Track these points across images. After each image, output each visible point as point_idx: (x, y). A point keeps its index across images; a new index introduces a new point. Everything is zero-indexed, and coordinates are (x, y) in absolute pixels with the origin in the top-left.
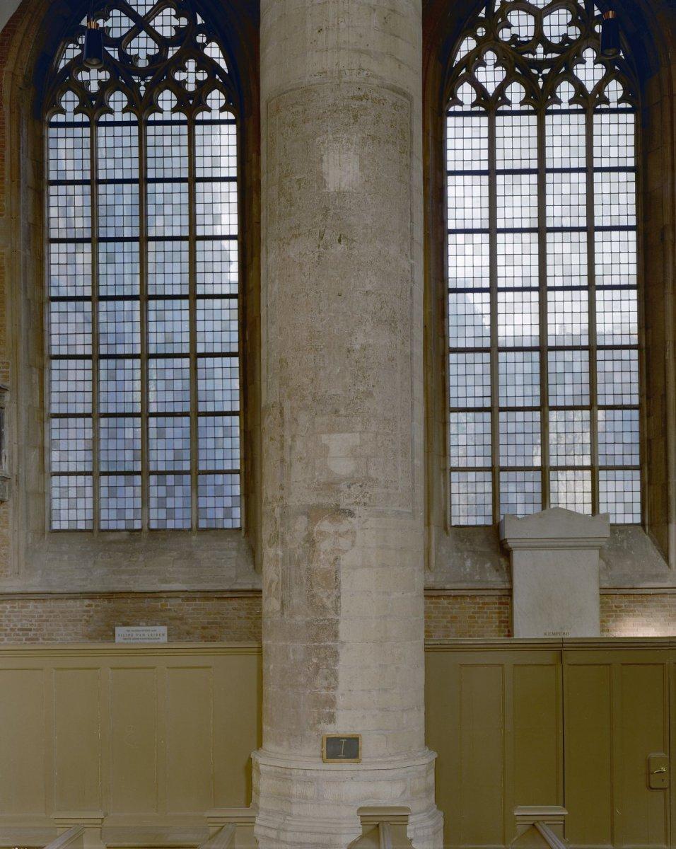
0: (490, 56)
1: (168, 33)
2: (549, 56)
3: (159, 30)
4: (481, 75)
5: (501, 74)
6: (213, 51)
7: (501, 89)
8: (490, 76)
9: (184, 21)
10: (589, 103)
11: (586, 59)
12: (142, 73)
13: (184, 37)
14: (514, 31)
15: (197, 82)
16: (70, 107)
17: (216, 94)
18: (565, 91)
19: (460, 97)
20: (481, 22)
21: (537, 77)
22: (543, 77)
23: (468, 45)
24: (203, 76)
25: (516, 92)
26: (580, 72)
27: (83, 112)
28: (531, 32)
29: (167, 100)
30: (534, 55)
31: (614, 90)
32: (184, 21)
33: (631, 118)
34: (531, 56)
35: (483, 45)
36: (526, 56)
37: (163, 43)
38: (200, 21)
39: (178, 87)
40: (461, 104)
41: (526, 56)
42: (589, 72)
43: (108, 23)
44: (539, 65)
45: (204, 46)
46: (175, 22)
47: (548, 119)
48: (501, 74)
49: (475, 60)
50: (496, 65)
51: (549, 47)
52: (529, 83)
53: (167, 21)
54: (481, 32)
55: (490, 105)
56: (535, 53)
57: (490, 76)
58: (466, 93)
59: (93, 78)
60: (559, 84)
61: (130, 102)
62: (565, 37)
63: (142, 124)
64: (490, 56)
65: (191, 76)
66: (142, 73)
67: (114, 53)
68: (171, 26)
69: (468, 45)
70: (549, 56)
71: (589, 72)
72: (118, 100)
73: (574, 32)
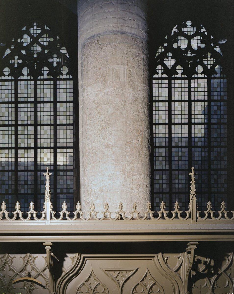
1: (45, 44)
2: (193, 55)
3: (42, 43)
6: (64, 51)
8: (170, 62)
9: (52, 40)
15: (57, 62)
16: (26, 73)
17: (26, 69)
20: (166, 41)
21: (188, 64)
23: (161, 50)
25: (180, 70)
27: (11, 76)
28: (186, 46)
34: (185, 55)
35: (167, 50)
42: (209, 62)
43: (22, 40)
46: (48, 40)
47: (58, 82)
49: (164, 55)
50: (172, 58)
51: (193, 51)
52: (185, 66)
53: (45, 39)
56: (187, 54)
59: (16, 61)
60: (43, 67)
63: (55, 80)
65: (55, 60)
67: (24, 52)
68: (47, 41)
69: (161, 50)
70: (193, 55)
71: (209, 62)
72: (26, 71)
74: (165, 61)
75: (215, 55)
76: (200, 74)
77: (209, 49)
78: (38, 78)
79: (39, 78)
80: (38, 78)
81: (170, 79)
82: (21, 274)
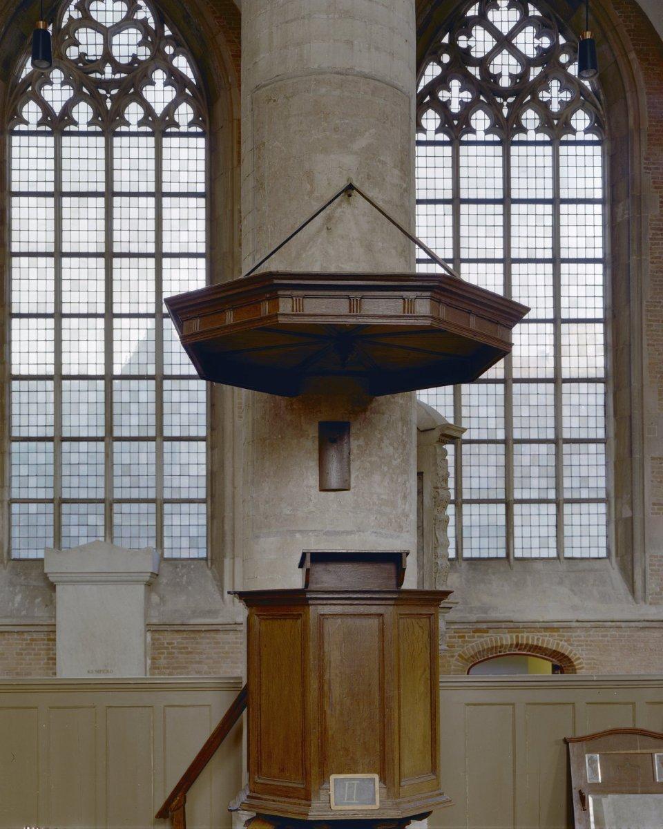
2: (118, 76)
4: (48, 93)
5: (68, 93)
7: (68, 107)
8: (57, 94)
10: (160, 126)
11: (156, 81)
14: (82, 49)
18: (134, 112)
19: (25, 116)
25: (83, 113)
26: (149, 94)
30: (102, 74)
31: (185, 113)
33: (201, 142)
34: (98, 76)
36: (93, 75)
40: (27, 123)
41: (93, 75)
42: (159, 94)
44: (108, 84)
47: (117, 141)
48: (68, 93)
50: (63, 84)
51: (117, 68)
52: (96, 102)
55: (57, 124)
56: (103, 73)
57: (57, 94)
58: (31, 112)
60: (127, 105)
62: (135, 57)
70: (118, 76)
71: (159, 94)
73: (144, 53)
74: (468, 98)
75: (175, 78)
76: (583, 133)
77: (159, 60)
78: (462, 139)
79: (564, 138)
80: (462, 139)
81: (455, 143)
82: (141, 578)
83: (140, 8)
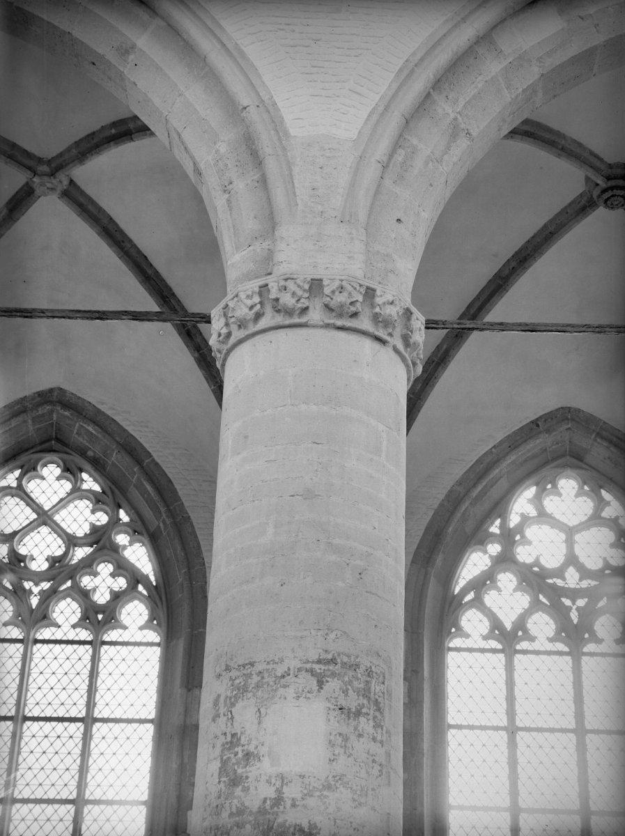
0: (507, 580)
5: (524, 600)
9: (102, 518)
12: (38, 577)
13: (100, 540)
22: (578, 609)
24: (121, 583)
25: (543, 625)
29: (67, 611)
32: (102, 518)
36: (550, 581)
37: (71, 541)
38: (124, 516)
39: (84, 596)
44: (574, 594)
45: (125, 547)
51: (584, 573)
52: (559, 613)
54: (494, 549)
58: (472, 622)
61: (17, 614)
64: (507, 580)
66: (38, 577)
69: (475, 564)
83: (608, 503)
